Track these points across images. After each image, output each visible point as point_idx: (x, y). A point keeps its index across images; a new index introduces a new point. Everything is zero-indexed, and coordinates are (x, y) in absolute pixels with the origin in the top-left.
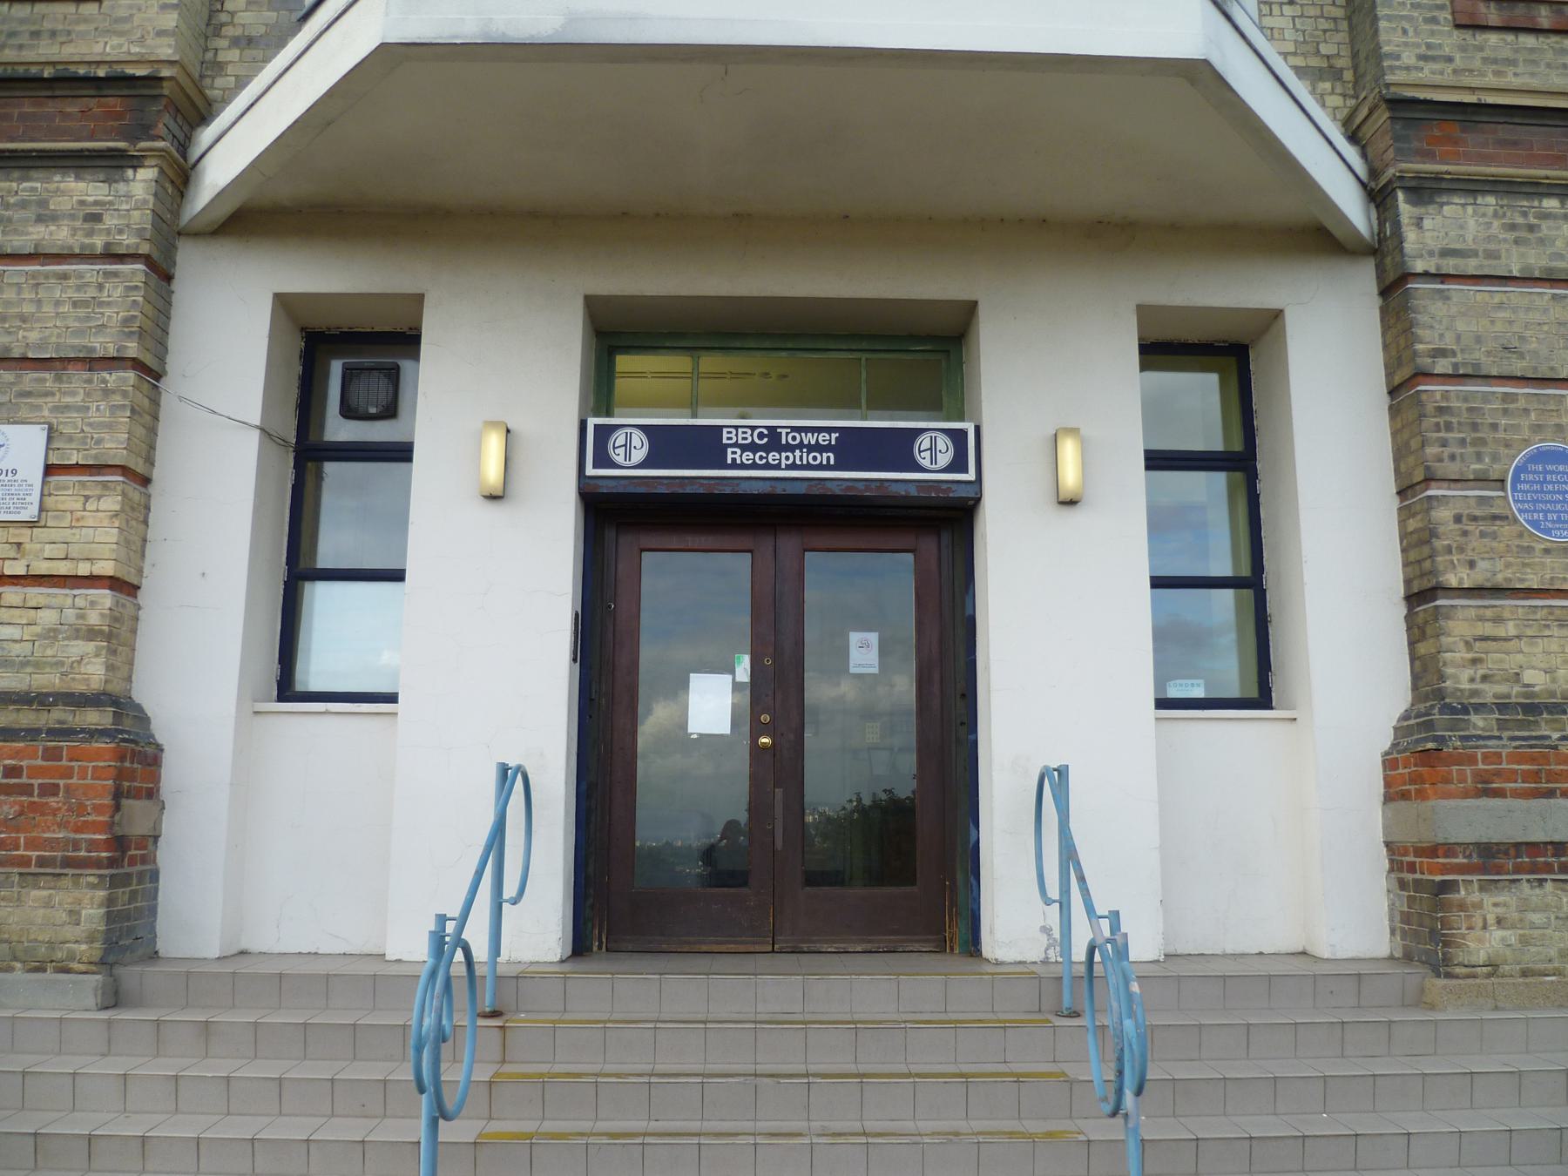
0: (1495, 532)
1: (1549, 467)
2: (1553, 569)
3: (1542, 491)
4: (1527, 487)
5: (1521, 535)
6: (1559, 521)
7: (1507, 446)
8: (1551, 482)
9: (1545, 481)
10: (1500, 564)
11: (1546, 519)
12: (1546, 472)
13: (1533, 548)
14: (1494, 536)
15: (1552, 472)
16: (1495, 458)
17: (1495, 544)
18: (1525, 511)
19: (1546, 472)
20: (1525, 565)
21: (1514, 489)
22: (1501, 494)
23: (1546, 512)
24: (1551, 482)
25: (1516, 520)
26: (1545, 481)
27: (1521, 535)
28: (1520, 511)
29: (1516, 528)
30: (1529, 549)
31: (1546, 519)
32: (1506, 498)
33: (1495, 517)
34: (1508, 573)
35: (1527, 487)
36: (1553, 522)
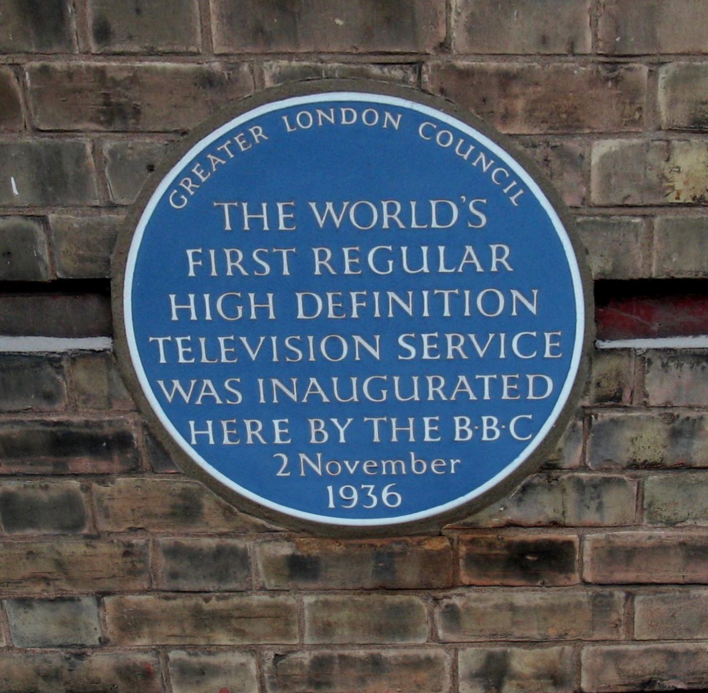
0: (70, 501)
1: (326, 213)
2: (326, 629)
3: (286, 322)
4: (214, 306)
5: (186, 510)
6: (359, 444)
7: (117, 112)
8: (336, 282)
9: (303, 277)
10: (95, 621)
11: (299, 441)
12: (305, 235)
13: (243, 558)
14: (70, 517)
15: (335, 237)
16: (55, 177)
17: (73, 548)
18: (208, 411)
19: (305, 235)
20: (204, 620)
21: (151, 318)
22: (101, 343)
23: (297, 415)
24: (336, 282)
25: (163, 452)
26: (303, 277)
27: (186, 510)
28: (176, 410)
29: (161, 486)
30: (226, 563)
31: (299, 441)
32: (114, 359)
33: (65, 443)
34: (138, 651)
35: (214, 306)
36: (332, 451)
